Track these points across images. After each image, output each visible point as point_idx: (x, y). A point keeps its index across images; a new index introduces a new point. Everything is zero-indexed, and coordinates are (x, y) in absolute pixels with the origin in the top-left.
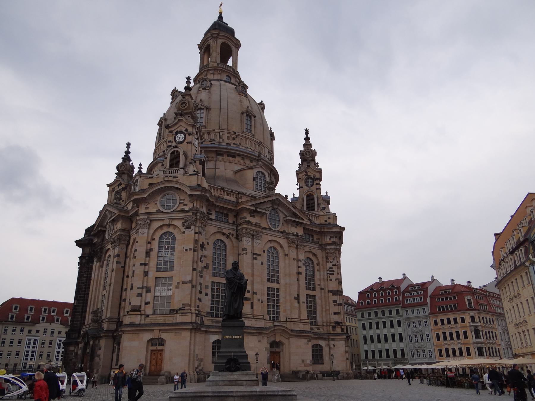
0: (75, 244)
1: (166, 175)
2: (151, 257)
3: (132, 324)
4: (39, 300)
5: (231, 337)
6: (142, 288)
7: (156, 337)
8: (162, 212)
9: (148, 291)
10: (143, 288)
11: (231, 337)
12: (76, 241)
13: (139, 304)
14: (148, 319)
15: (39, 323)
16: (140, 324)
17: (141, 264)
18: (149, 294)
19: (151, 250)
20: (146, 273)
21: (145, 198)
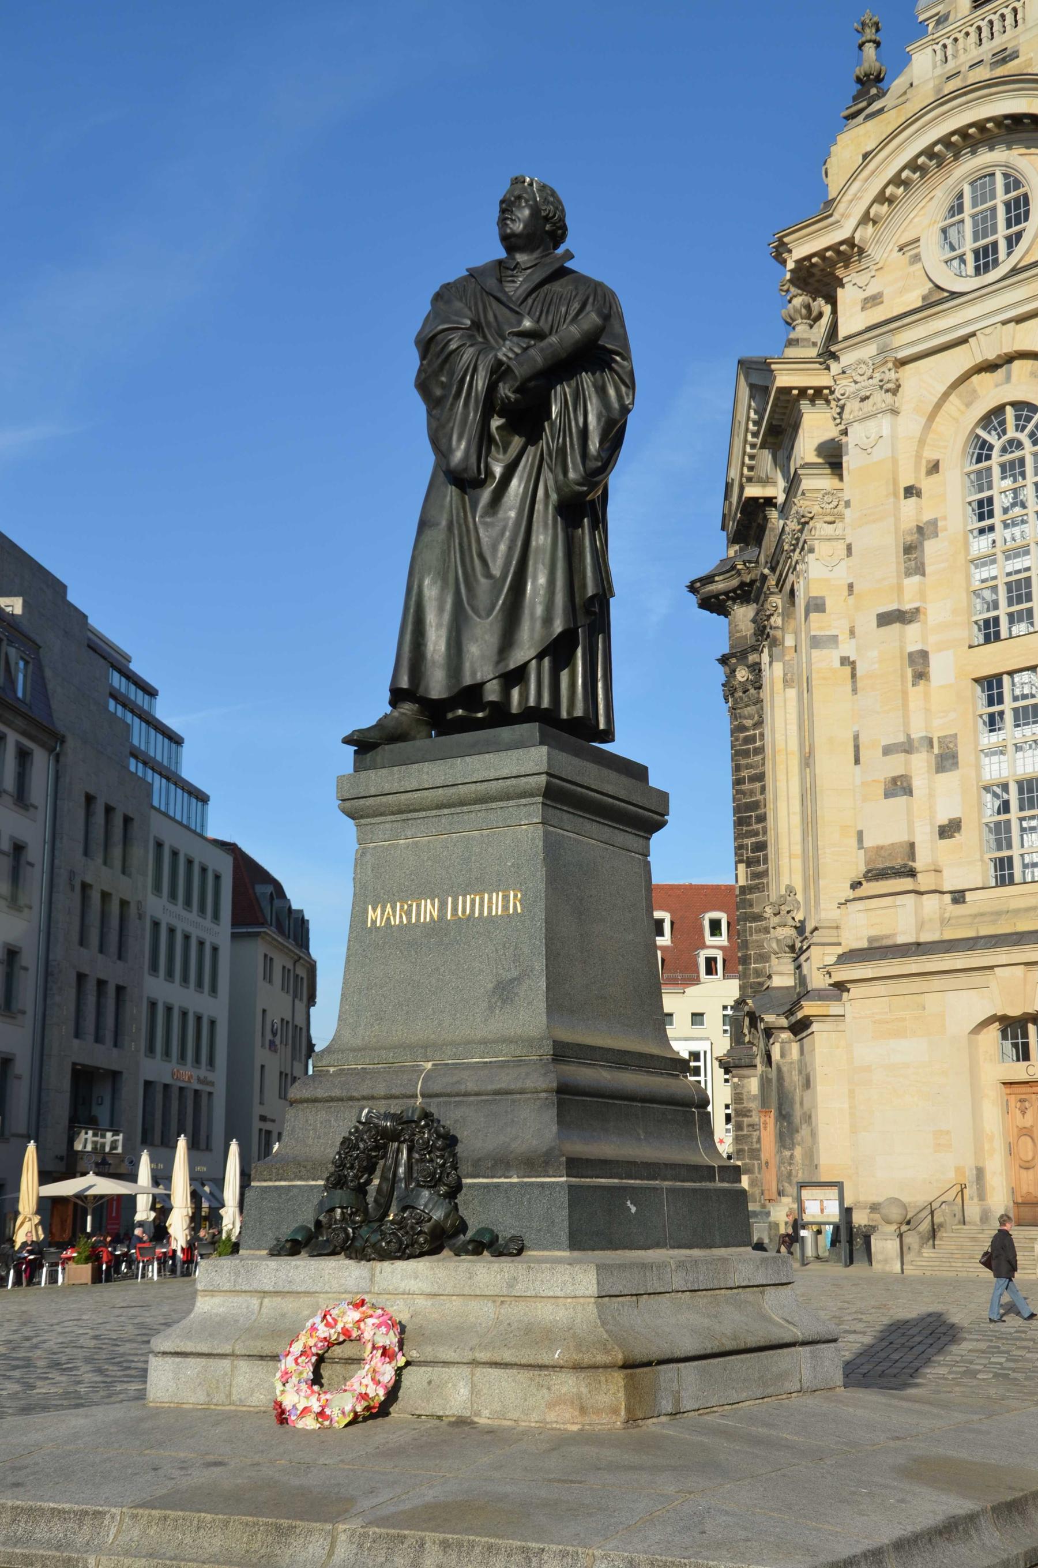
0: (693, 600)
1: (951, 64)
2: (928, 570)
3: (878, 951)
4: (691, 887)
5: (429, 910)
6: (907, 747)
7: (1014, 1012)
8: (954, 295)
9: (947, 760)
10: (907, 747)
11: (429, 910)
12: (692, 588)
13: (905, 838)
14: (960, 909)
15: (696, 981)
16: (918, 944)
17: (885, 619)
18: (948, 780)
19: (924, 531)
20: (919, 665)
21: (850, 242)
